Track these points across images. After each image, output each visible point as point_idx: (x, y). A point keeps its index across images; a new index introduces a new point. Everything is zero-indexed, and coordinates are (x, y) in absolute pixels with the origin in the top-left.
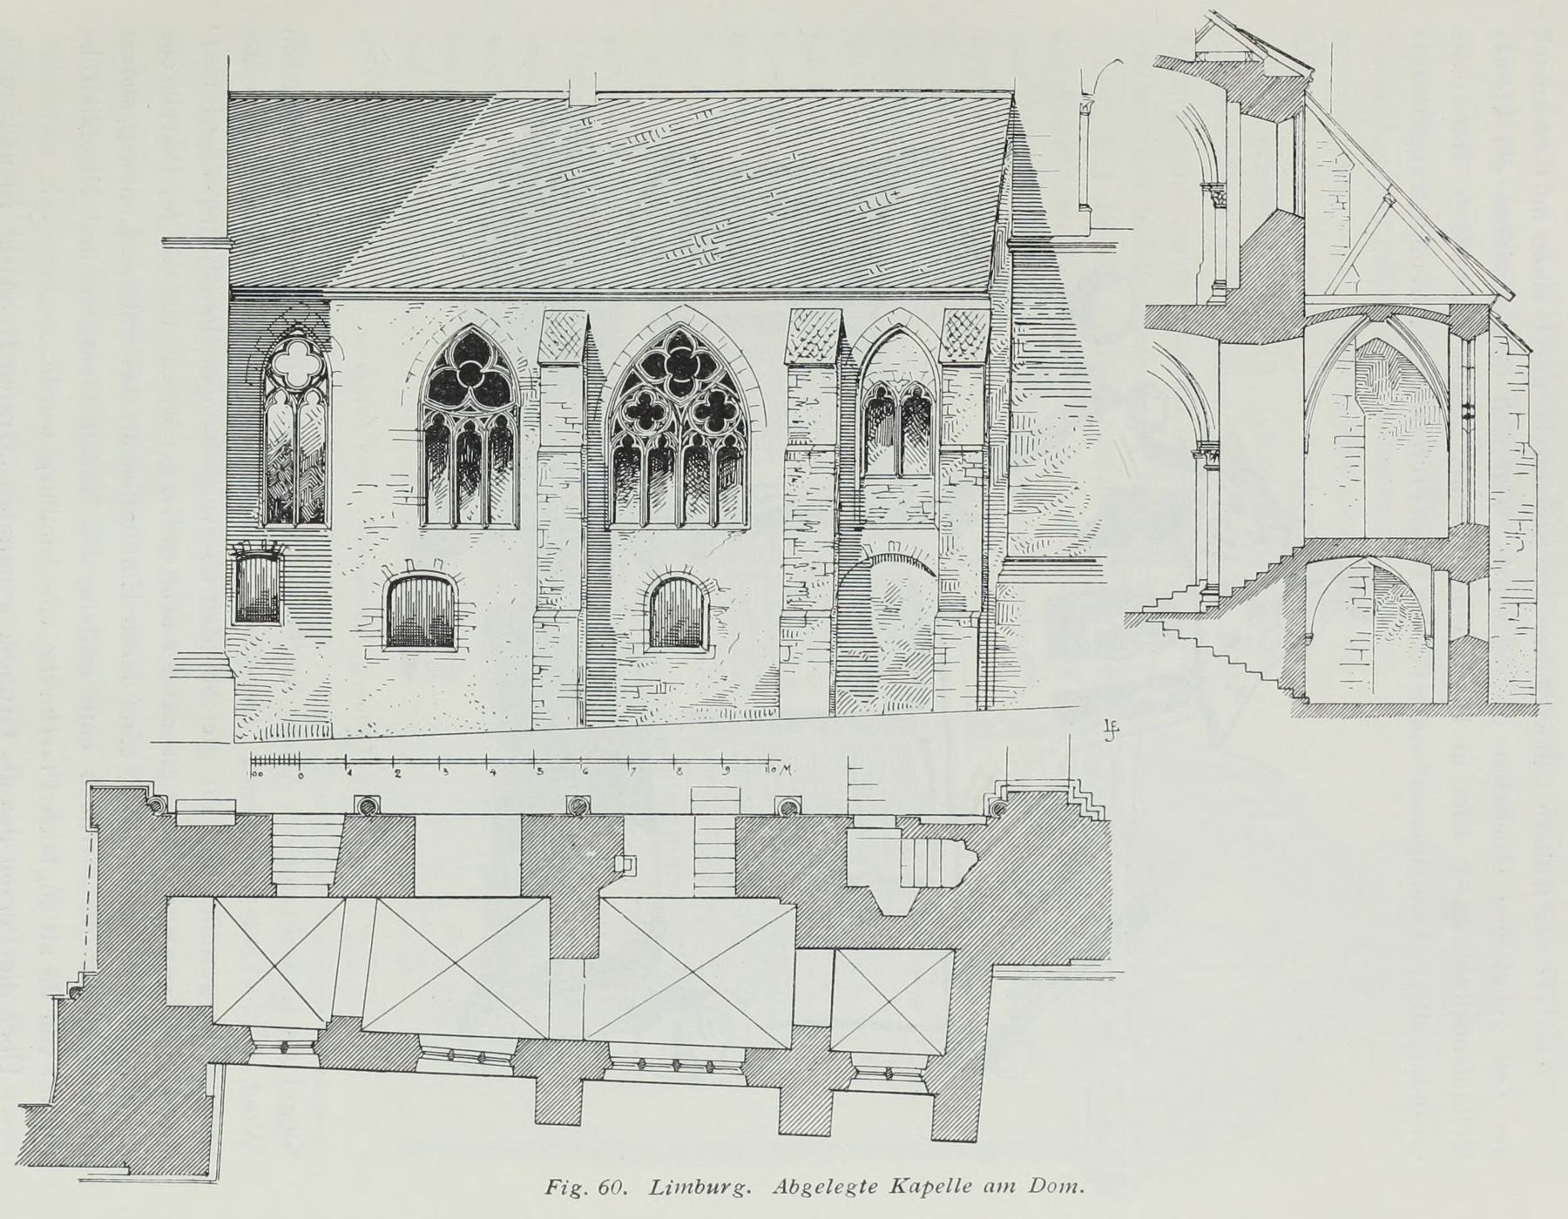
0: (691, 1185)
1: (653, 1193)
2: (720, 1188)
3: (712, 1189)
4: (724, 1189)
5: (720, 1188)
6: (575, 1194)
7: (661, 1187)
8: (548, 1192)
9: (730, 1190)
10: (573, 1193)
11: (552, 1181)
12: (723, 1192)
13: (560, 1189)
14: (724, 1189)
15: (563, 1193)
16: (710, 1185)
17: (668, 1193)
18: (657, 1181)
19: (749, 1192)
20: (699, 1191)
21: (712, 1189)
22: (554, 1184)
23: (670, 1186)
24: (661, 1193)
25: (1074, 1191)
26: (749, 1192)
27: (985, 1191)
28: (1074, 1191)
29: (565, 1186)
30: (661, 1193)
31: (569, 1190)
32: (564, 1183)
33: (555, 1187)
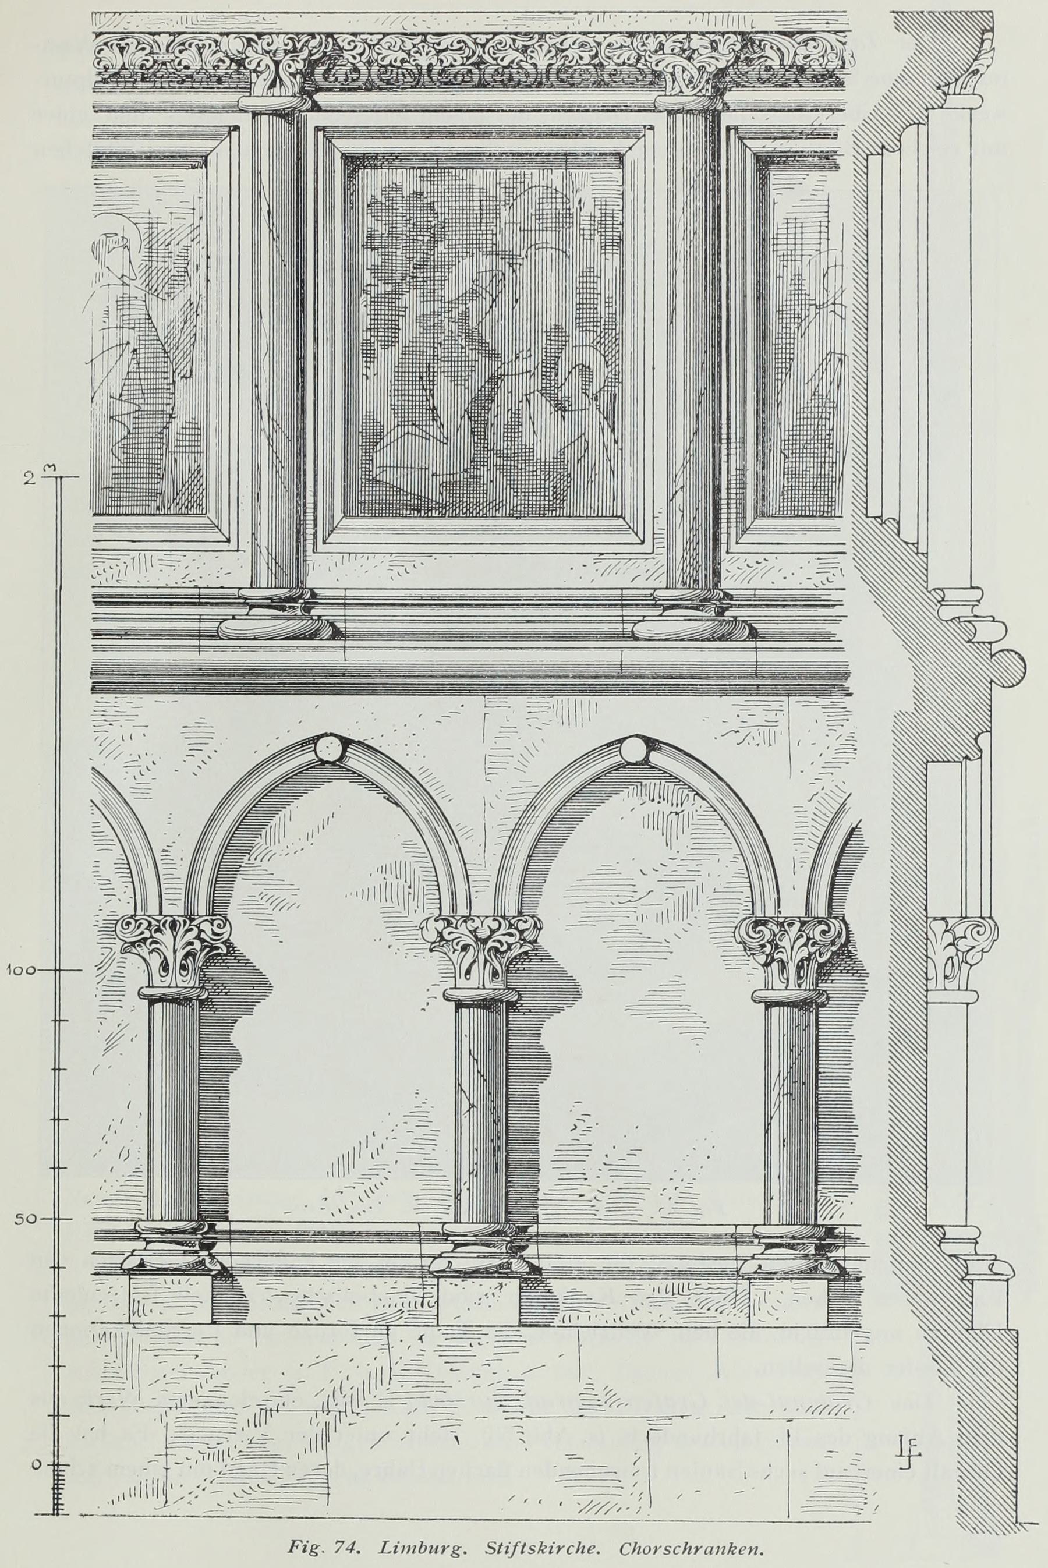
0: (415, 1547)
1: (382, 1552)
2: (440, 1550)
3: (434, 1550)
4: (444, 1550)
5: (440, 1550)
6: (314, 1552)
7: (390, 1547)
8: (291, 1551)
9: (449, 1551)
10: (312, 1551)
11: (294, 1542)
12: (442, 1553)
13: (301, 1548)
14: (444, 1550)
15: (304, 1551)
16: (432, 1547)
17: (395, 1552)
18: (385, 1542)
19: (465, 1553)
20: (422, 1551)
21: (434, 1550)
22: (296, 1544)
23: (396, 1547)
24: (389, 1552)
25: (755, 1554)
26: (465, 1553)
27: (705, 1553)
28: (755, 1554)
29: (305, 1546)
30: (389, 1552)
31: (308, 1549)
32: (305, 1543)
33: (297, 1547)
